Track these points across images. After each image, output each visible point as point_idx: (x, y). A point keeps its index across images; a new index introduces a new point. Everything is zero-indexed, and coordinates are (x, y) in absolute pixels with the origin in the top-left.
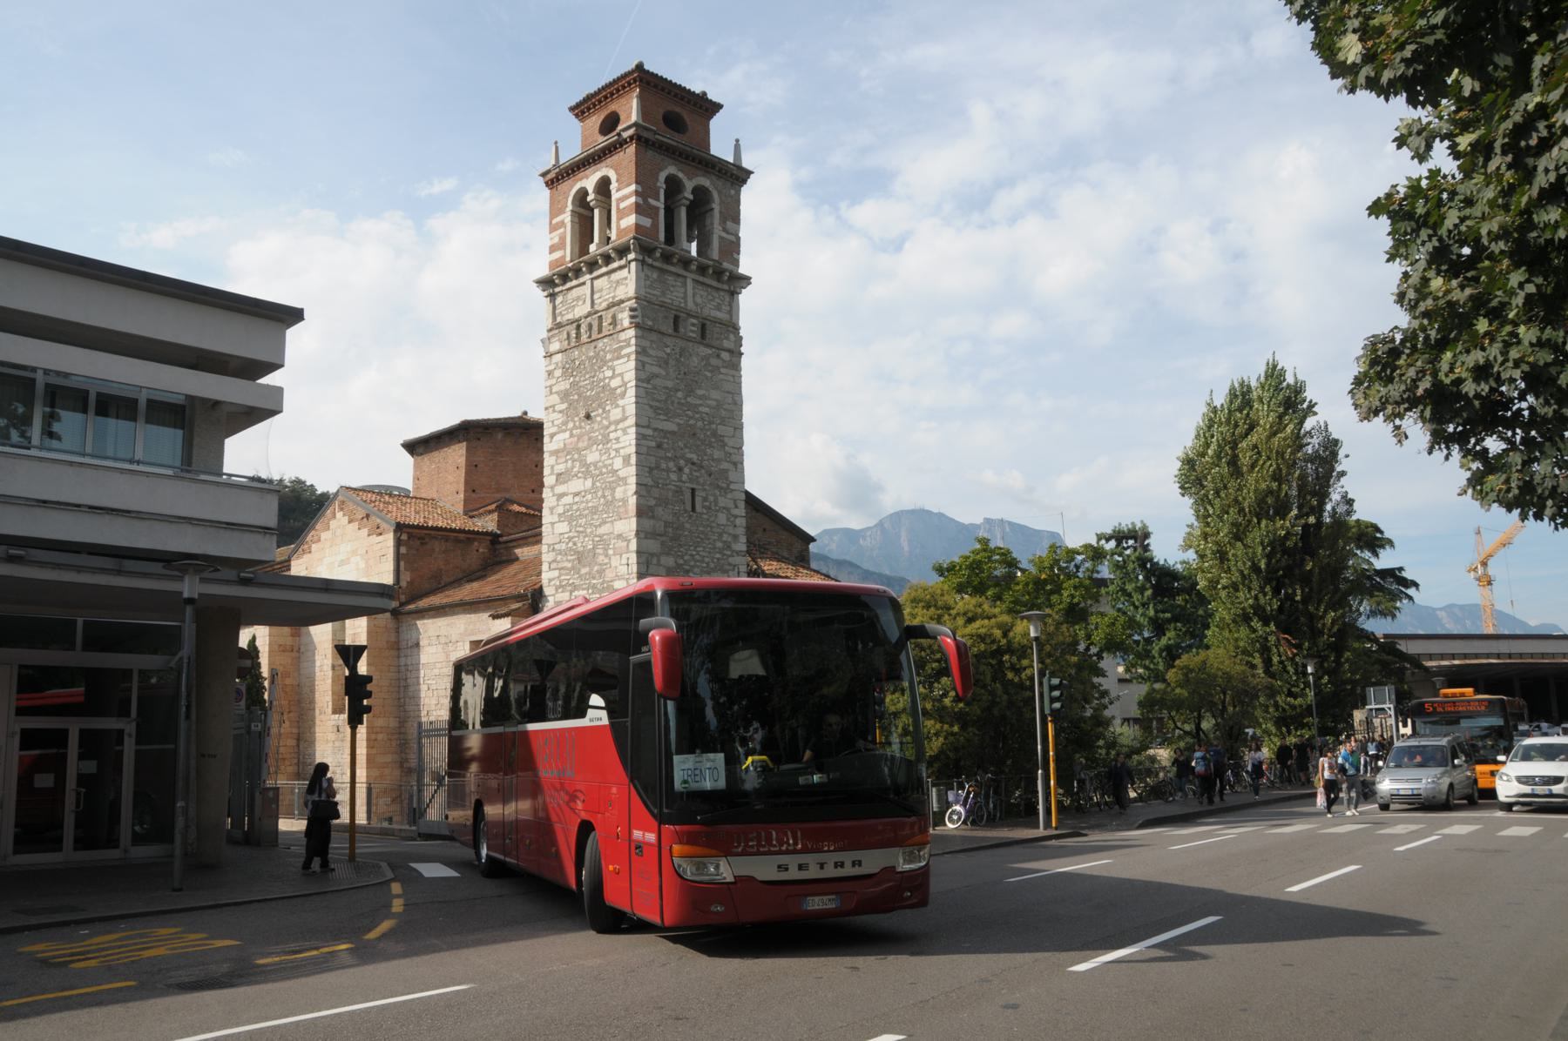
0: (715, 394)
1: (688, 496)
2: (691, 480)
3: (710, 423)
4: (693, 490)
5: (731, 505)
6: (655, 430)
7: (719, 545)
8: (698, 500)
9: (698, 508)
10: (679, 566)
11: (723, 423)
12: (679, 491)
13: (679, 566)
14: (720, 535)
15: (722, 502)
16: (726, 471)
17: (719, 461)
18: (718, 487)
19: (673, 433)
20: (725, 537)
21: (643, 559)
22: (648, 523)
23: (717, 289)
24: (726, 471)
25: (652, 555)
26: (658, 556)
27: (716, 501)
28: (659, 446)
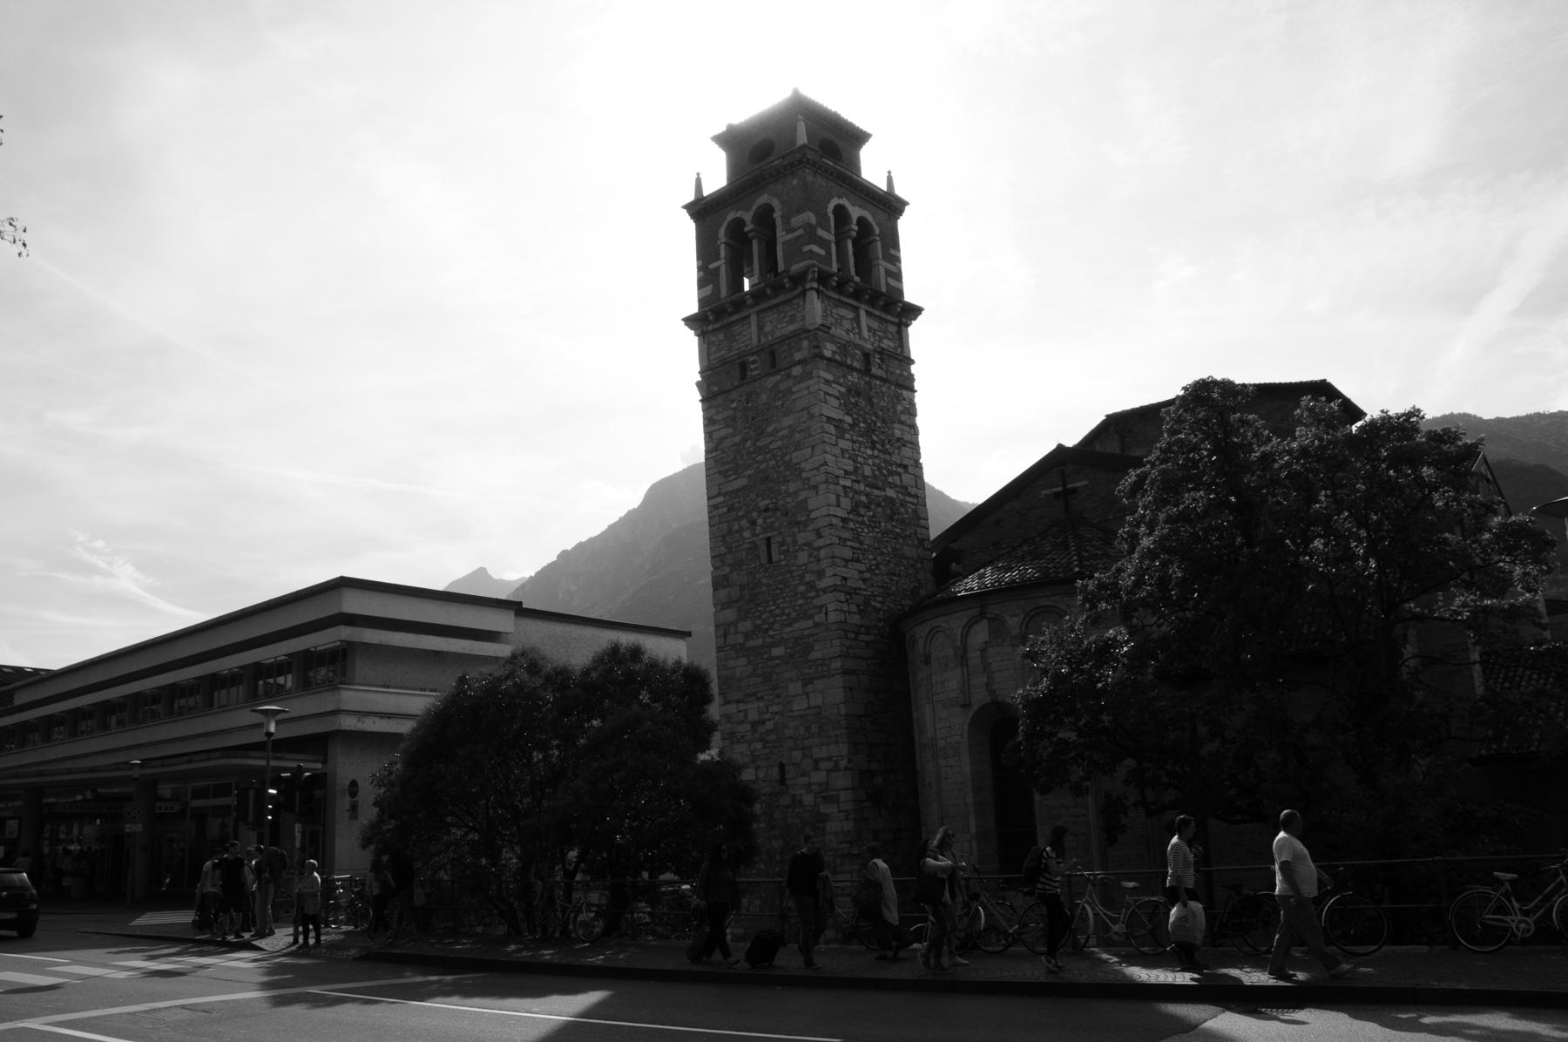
0: (787, 421)
1: (763, 548)
2: (765, 530)
3: (784, 455)
4: (768, 539)
5: (811, 536)
6: (725, 494)
7: (802, 588)
8: (774, 547)
9: (775, 557)
10: (757, 627)
11: (798, 447)
12: (754, 546)
13: (757, 627)
14: (802, 577)
15: (802, 538)
16: (805, 501)
17: (796, 493)
18: (797, 523)
19: (744, 487)
20: (808, 578)
21: (721, 632)
22: (723, 594)
23: (790, 300)
24: (805, 501)
25: (729, 625)
26: (734, 624)
27: (795, 542)
28: (731, 508)
